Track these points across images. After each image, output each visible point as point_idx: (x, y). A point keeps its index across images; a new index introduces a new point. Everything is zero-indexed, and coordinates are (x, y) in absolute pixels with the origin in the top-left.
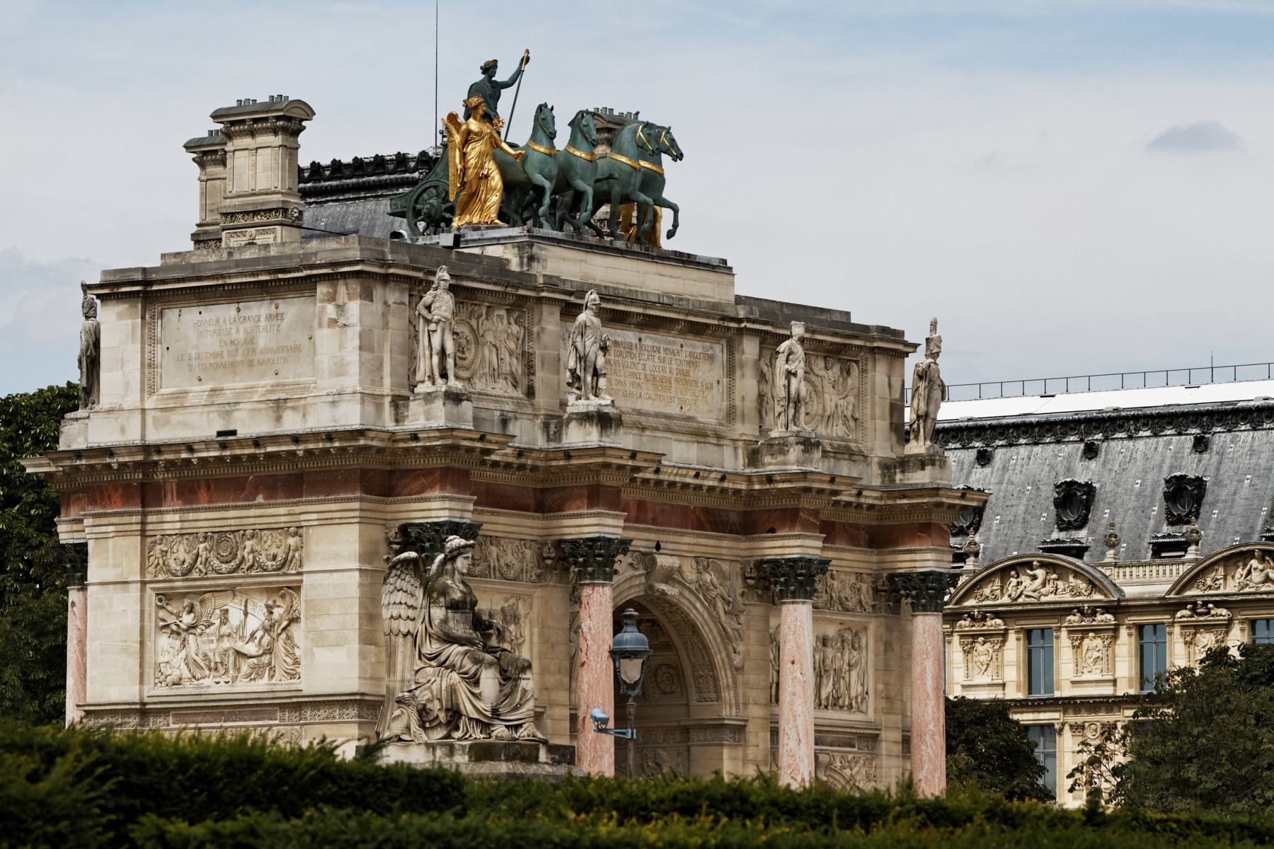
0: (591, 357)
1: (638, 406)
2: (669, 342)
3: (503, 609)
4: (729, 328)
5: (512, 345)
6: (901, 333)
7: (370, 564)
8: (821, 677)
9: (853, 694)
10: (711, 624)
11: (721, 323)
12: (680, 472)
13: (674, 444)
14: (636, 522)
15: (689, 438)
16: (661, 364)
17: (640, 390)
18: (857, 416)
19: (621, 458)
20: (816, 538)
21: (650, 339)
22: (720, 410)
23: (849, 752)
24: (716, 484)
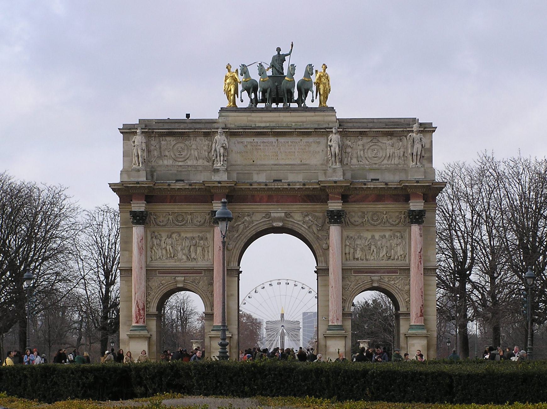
0: (218, 150)
1: (276, 163)
3: (199, 236)
5: (205, 148)
7: (125, 225)
8: (380, 249)
9: (399, 255)
11: (316, 130)
12: (279, 184)
13: (289, 174)
15: (299, 172)
18: (406, 156)
19: (214, 184)
21: (282, 139)
23: (394, 275)
24: (302, 187)
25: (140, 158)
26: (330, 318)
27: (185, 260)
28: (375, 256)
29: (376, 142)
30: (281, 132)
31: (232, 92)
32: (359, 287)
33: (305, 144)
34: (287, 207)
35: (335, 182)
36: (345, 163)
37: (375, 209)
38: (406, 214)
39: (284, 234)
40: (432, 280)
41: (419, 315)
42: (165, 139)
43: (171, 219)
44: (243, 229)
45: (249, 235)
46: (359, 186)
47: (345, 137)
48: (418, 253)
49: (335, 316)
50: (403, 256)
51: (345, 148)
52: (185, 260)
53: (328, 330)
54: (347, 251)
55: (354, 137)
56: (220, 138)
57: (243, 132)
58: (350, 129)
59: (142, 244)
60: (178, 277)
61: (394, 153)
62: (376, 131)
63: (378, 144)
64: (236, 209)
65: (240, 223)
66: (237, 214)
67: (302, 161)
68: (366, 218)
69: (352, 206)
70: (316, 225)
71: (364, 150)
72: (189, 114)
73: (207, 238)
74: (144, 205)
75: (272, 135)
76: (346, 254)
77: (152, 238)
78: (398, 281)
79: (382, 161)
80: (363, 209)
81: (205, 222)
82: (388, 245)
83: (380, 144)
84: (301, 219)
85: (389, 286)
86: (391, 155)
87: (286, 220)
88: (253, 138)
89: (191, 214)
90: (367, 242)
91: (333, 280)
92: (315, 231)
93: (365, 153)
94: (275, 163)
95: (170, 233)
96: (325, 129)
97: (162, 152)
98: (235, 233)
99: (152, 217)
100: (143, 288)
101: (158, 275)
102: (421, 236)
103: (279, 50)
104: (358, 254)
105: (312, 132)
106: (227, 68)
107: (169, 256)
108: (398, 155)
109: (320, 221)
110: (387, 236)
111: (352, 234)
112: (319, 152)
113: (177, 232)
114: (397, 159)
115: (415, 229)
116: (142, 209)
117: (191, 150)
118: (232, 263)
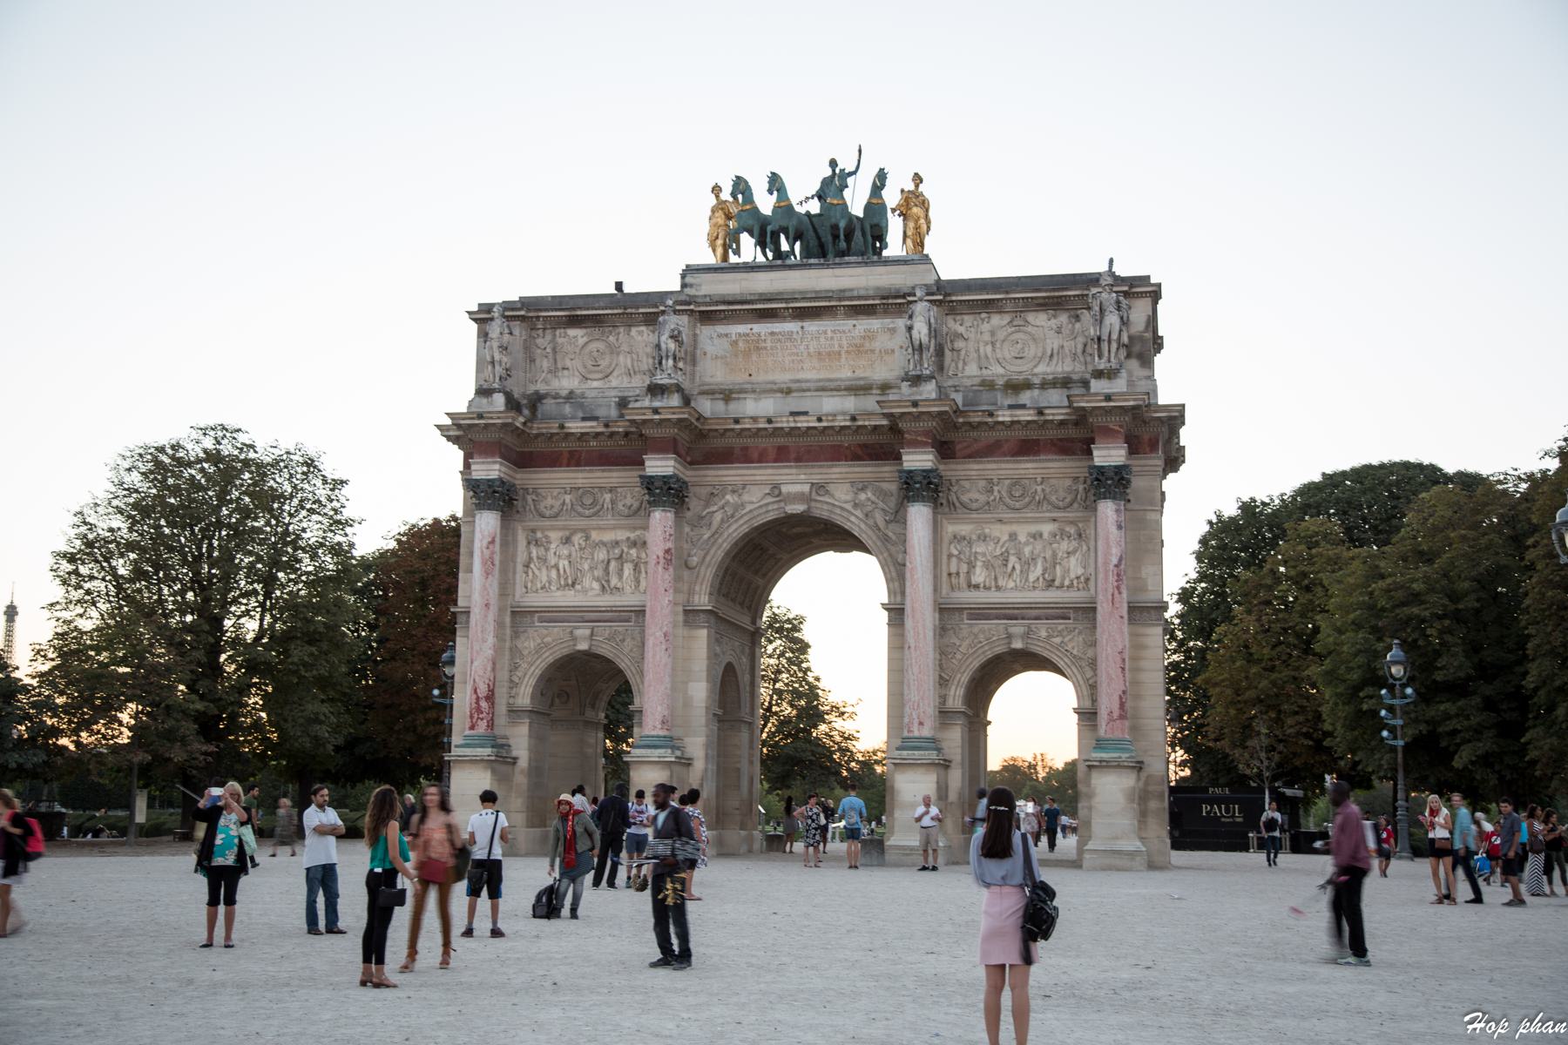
0: (663, 346)
1: (801, 376)
2: (839, 325)
3: (628, 539)
4: (900, 304)
5: (649, 350)
6: (1149, 277)
9: (1073, 576)
10: (870, 532)
11: (884, 301)
12: (797, 419)
13: (825, 399)
14: (775, 461)
19: (644, 414)
20: (925, 453)
21: (812, 326)
24: (848, 423)
25: (497, 367)
26: (906, 720)
27: (598, 592)
28: (1018, 580)
29: (1022, 323)
30: (808, 307)
32: (980, 651)
34: (816, 470)
35: (915, 404)
36: (951, 373)
37: (1017, 472)
38: (1089, 482)
39: (854, 552)
40: (1147, 635)
41: (1116, 715)
42: (565, 333)
43: (568, 501)
44: (722, 520)
45: (736, 534)
46: (977, 419)
48: (1111, 567)
49: (915, 716)
50: (1082, 578)
51: (951, 341)
52: (598, 592)
53: (898, 749)
54: (953, 570)
55: (971, 317)
56: (672, 321)
57: (728, 311)
59: (493, 553)
60: (579, 628)
61: (1062, 347)
62: (1018, 299)
64: (709, 479)
65: (715, 508)
66: (709, 489)
68: (996, 493)
69: (967, 466)
70: (883, 510)
71: (993, 344)
73: (645, 543)
74: (497, 467)
75: (790, 316)
76: (950, 574)
77: (529, 543)
78: (1070, 637)
79: (1035, 366)
80: (989, 472)
81: (641, 506)
82: (1048, 554)
83: (1029, 329)
84: (849, 498)
85: (1048, 647)
86: (1055, 351)
87: (816, 501)
88: (750, 326)
89: (611, 490)
90: (998, 548)
91: (912, 632)
92: (881, 524)
93: (997, 351)
95: (567, 533)
96: (904, 296)
97: (558, 357)
98: (704, 530)
99: (529, 498)
100: (491, 652)
101: (537, 624)
102: (1119, 527)
103: (833, 163)
104: (979, 576)
107: (562, 583)
108: (1070, 351)
109: (892, 502)
110: (1046, 536)
111: (964, 529)
112: (893, 351)
113: (583, 530)
114: (1068, 360)
115: (1108, 510)
116: (494, 475)
117: (618, 354)
118: (696, 597)
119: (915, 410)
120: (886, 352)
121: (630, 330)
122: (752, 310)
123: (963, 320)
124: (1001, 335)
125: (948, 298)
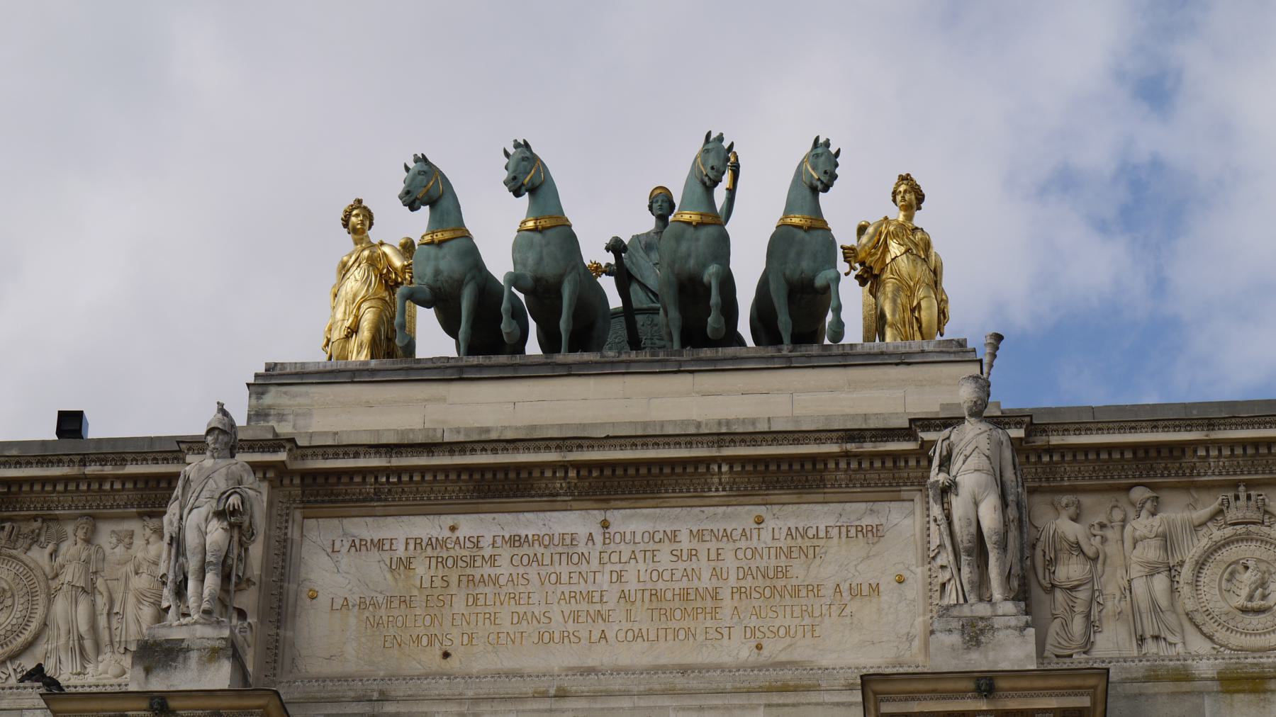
0: (191, 539)
4: (895, 456)
11: (852, 447)
15: (737, 700)
16: (681, 565)
17: (601, 625)
22: (910, 638)
29: (1256, 516)
30: (625, 464)
31: (365, 333)
33: (784, 543)
35: (986, 684)
47: (1048, 498)
55: (1105, 500)
57: (388, 471)
58: (1078, 431)
62: (1244, 443)
63: (1263, 528)
67: (765, 643)
71: (1172, 571)
72: (79, 415)
75: (570, 491)
88: (448, 520)
93: (1185, 590)
94: (590, 662)
96: (907, 433)
105: (825, 457)
106: (346, 225)
112: (875, 589)
119: (983, 705)
120: (856, 592)
121: (94, 530)
122: (460, 469)
123: (1079, 506)
124: (1192, 550)
125: (1040, 441)
